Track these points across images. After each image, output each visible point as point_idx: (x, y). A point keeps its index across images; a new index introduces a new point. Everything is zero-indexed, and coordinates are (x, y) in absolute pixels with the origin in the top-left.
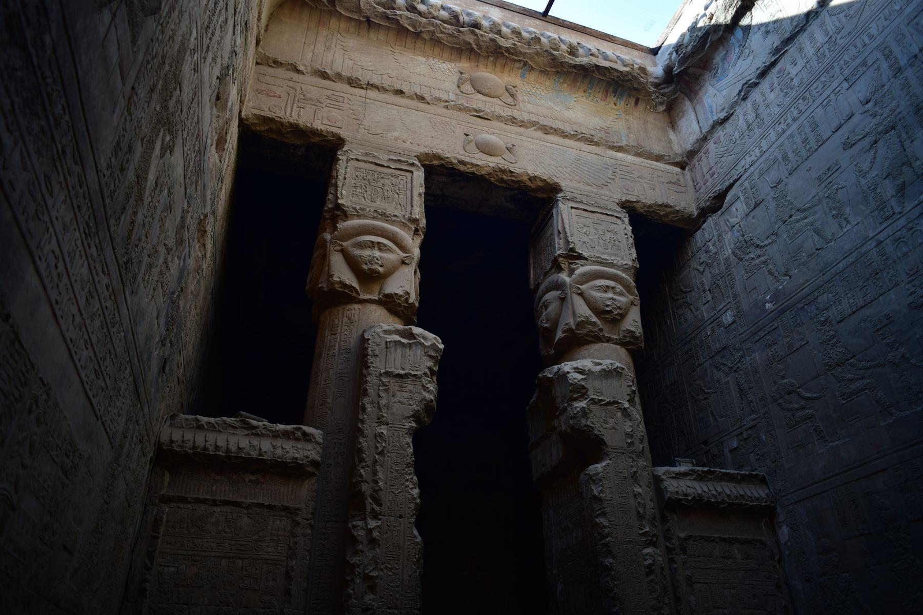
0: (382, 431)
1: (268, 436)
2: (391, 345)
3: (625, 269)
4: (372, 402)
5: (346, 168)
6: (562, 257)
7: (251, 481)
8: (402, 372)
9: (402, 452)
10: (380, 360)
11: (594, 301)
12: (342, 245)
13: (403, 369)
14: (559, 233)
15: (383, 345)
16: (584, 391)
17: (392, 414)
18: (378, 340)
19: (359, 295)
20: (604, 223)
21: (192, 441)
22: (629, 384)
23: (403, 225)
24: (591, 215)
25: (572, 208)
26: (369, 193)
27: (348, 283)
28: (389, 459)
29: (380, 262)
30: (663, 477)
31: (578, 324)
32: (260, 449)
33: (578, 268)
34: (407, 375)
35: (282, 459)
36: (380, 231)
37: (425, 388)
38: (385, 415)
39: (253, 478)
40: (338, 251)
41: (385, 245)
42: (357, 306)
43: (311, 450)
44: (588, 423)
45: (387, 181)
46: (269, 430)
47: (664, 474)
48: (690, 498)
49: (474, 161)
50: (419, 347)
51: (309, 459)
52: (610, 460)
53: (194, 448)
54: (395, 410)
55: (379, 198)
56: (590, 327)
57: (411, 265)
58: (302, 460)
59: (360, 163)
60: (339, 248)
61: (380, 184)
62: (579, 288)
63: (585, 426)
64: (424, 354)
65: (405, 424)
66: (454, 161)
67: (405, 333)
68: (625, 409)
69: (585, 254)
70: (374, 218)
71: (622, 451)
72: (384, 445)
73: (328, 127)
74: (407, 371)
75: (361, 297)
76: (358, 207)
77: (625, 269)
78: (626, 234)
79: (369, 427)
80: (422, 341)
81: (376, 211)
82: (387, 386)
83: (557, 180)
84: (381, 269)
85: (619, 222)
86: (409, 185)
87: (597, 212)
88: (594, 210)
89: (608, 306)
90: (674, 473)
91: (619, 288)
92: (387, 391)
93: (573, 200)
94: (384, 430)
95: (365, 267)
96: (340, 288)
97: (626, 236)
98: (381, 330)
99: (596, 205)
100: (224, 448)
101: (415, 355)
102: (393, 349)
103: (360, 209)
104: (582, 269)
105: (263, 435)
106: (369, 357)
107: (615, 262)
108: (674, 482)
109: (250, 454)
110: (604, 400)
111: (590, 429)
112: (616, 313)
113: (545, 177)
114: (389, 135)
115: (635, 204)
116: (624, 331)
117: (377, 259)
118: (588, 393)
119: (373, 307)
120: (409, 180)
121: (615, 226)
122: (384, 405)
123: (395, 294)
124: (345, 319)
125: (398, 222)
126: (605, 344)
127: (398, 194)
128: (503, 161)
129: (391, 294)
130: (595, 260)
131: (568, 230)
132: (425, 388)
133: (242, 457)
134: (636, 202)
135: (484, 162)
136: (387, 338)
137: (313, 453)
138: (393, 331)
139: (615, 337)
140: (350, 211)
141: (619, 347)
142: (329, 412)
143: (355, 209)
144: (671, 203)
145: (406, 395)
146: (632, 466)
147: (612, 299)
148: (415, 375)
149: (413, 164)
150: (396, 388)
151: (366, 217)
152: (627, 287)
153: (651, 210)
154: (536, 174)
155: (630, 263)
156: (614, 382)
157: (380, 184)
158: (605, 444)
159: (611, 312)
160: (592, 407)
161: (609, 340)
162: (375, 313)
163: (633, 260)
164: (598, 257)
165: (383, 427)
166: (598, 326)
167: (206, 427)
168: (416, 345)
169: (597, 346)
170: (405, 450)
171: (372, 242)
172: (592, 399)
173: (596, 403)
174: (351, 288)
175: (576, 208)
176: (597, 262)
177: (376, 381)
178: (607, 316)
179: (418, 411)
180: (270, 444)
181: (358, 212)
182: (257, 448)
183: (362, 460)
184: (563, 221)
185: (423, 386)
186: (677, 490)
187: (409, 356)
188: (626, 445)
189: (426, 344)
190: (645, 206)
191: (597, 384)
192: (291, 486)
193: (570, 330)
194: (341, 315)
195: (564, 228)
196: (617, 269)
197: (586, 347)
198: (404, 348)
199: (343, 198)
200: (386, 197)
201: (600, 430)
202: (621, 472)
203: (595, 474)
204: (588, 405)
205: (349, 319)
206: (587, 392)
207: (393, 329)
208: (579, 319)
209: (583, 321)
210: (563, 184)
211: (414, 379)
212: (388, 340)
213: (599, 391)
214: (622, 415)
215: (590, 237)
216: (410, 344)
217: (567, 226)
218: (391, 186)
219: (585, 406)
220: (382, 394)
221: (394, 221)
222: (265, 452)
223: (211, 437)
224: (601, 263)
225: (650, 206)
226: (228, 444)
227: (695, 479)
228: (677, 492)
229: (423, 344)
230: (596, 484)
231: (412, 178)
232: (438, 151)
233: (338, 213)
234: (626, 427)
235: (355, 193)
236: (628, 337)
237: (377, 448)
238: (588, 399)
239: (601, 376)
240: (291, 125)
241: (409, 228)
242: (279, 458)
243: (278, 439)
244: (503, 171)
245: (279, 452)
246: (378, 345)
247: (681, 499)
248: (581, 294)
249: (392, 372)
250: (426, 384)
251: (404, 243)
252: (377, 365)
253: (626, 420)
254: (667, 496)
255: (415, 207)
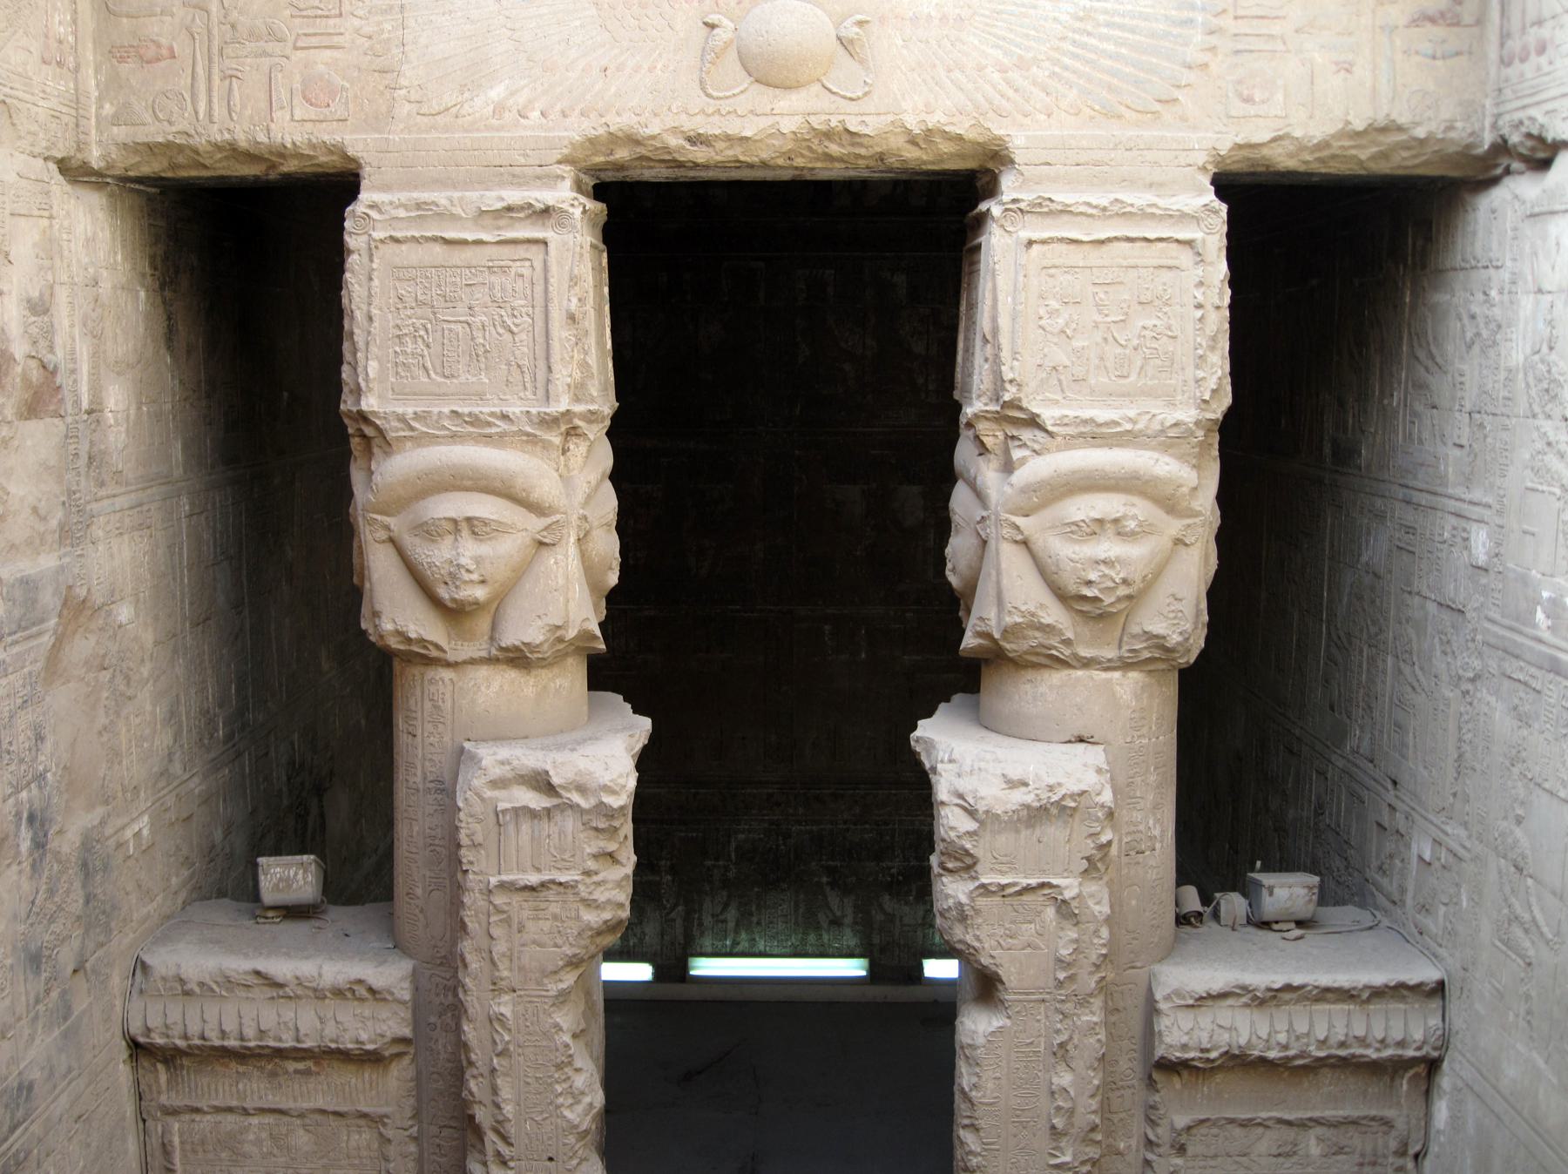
0: (503, 1010)
1: (308, 997)
2: (508, 818)
3: (1168, 440)
4: (478, 950)
5: (371, 279)
6: (986, 418)
7: (296, 1072)
8: (533, 879)
9: (544, 1043)
10: (488, 856)
11: (1053, 568)
12: (387, 528)
13: (538, 870)
14: (986, 341)
15: (492, 817)
16: (969, 861)
17: (521, 969)
18: (478, 808)
19: (444, 651)
20: (1133, 274)
21: (180, 1021)
22: (1092, 831)
23: (532, 439)
24: (1095, 256)
25: (1030, 243)
26: (436, 348)
27: (413, 635)
28: (521, 1059)
29: (475, 577)
30: (1163, 1006)
31: (1005, 631)
32: (297, 1030)
33: (1023, 461)
34: (543, 885)
35: (337, 1042)
36: (471, 479)
37: (590, 904)
38: (505, 974)
39: (301, 1066)
40: (384, 542)
41: (485, 522)
42: (446, 674)
43: (388, 1019)
44: (969, 938)
45: (480, 295)
46: (306, 987)
47: (1168, 998)
48: (1213, 1055)
49: (734, 127)
50: (569, 812)
51: (386, 1040)
52: (1009, 1017)
53: (186, 1037)
54: (525, 960)
55: (464, 360)
56: (1037, 634)
57: (564, 542)
58: (372, 1041)
59: (404, 247)
60: (382, 535)
61: (461, 309)
62: (1017, 528)
63: (960, 941)
64: (582, 828)
65: (549, 987)
66: (674, 142)
67: (537, 781)
68: (1064, 901)
69: (1048, 415)
70: (454, 437)
71: (1041, 997)
72: (507, 1038)
73: (309, 126)
74: (546, 877)
75: (451, 657)
76: (410, 410)
77: (1168, 440)
78: (1199, 306)
79: (475, 997)
80: (576, 798)
81: (453, 412)
82: (504, 912)
83: (999, 129)
84: (480, 593)
85: (1185, 257)
86: (539, 289)
87: (1117, 239)
88: (1103, 236)
89: (1089, 583)
90: (1191, 997)
91: (1136, 509)
92: (507, 921)
93: (1043, 209)
94: (505, 1006)
95: (443, 593)
96: (399, 642)
97: (1199, 313)
98: (483, 780)
99: (1116, 208)
100: (235, 1033)
101: (561, 833)
102: (511, 828)
103: (417, 416)
104: (1037, 467)
105: (298, 997)
106: (463, 852)
107: (1140, 426)
108: (1186, 1020)
109: (280, 1040)
110: (1014, 884)
111: (971, 951)
112: (1108, 600)
113: (962, 127)
114: (478, 102)
115: (1265, 151)
116: (1134, 636)
117: (468, 571)
118: (978, 867)
119: (483, 672)
120: (538, 265)
121: (1166, 276)
122: (504, 955)
123: (524, 644)
124: (428, 705)
125: (515, 434)
126: (1080, 673)
127: (512, 332)
128: (826, 102)
129: (517, 649)
130: (1071, 430)
131: (1004, 340)
132: (590, 904)
133: (268, 1047)
134: (1274, 140)
135: (764, 123)
136: (497, 799)
137: (390, 1023)
138: (510, 780)
139: (1110, 653)
140: (394, 430)
141: (1117, 675)
142: (421, 916)
143: (402, 419)
144: (1403, 119)
145: (546, 925)
146: (1058, 1032)
147: (1104, 562)
148: (561, 884)
149: (546, 211)
150: (526, 914)
151: (433, 439)
152: (1168, 501)
153: (1325, 153)
154: (932, 121)
155: (1188, 415)
156: (1054, 833)
157: (461, 309)
158: (1002, 983)
159: (1096, 599)
160: (982, 902)
161: (1087, 663)
162: (488, 687)
163: (1205, 401)
164: (1085, 422)
165: (506, 998)
166: (1060, 632)
167: (197, 990)
168: (562, 811)
169: (1057, 677)
170: (551, 1039)
171: (455, 521)
172: (983, 886)
173: (994, 892)
174: (422, 641)
175: (1043, 242)
176: (1081, 435)
177: (482, 903)
178: (1086, 607)
179: (575, 955)
180: (313, 1012)
181: (412, 429)
182: (291, 1025)
183: (471, 1063)
184: (995, 300)
185: (583, 900)
186: (1185, 1039)
187: (549, 836)
188: (1051, 983)
189: (584, 804)
190: (1302, 148)
191: (1004, 841)
192: (367, 1075)
193: (987, 635)
194: (418, 683)
195: (995, 330)
196: (1144, 447)
197: (1029, 674)
198: (536, 821)
199: (370, 390)
200: (481, 351)
201: (993, 953)
202: (1032, 1043)
203: (970, 1045)
204: (972, 900)
205: (437, 707)
206: (975, 864)
207: (510, 775)
208: (1009, 620)
209: (1016, 624)
210: (1018, 142)
211: (561, 889)
212: (502, 806)
213: (1004, 859)
214: (1058, 911)
215: (1077, 344)
216: (548, 811)
217: (1004, 322)
218: (494, 311)
219: (964, 899)
220: (495, 932)
221: (502, 435)
222: (306, 1035)
223: (212, 1012)
224: (1095, 435)
225: (1321, 146)
226: (241, 1024)
227: (1247, 1005)
228: (1184, 1047)
229: (578, 806)
230: (970, 1065)
231: (545, 262)
232: (620, 122)
233: (369, 431)
234: (1061, 943)
235: (401, 358)
236: (1145, 648)
237: (494, 1042)
238: (977, 884)
239: (1019, 820)
240: (217, 147)
241: (546, 446)
242: (332, 1041)
243: (327, 1001)
244: (828, 135)
245: (330, 1031)
246: (480, 821)
247: (1193, 1059)
248: (1025, 543)
249: (512, 884)
250: (590, 893)
251: (535, 496)
252: (482, 870)
253: (1066, 924)
254: (1160, 1052)
255: (556, 367)
